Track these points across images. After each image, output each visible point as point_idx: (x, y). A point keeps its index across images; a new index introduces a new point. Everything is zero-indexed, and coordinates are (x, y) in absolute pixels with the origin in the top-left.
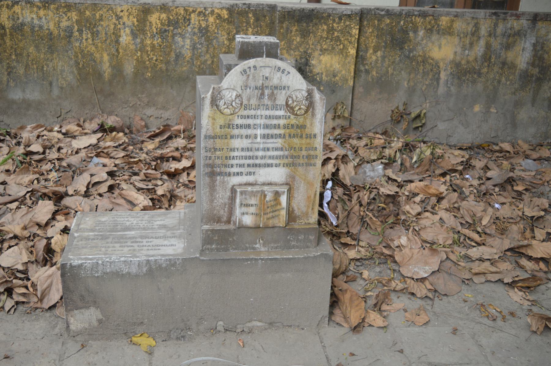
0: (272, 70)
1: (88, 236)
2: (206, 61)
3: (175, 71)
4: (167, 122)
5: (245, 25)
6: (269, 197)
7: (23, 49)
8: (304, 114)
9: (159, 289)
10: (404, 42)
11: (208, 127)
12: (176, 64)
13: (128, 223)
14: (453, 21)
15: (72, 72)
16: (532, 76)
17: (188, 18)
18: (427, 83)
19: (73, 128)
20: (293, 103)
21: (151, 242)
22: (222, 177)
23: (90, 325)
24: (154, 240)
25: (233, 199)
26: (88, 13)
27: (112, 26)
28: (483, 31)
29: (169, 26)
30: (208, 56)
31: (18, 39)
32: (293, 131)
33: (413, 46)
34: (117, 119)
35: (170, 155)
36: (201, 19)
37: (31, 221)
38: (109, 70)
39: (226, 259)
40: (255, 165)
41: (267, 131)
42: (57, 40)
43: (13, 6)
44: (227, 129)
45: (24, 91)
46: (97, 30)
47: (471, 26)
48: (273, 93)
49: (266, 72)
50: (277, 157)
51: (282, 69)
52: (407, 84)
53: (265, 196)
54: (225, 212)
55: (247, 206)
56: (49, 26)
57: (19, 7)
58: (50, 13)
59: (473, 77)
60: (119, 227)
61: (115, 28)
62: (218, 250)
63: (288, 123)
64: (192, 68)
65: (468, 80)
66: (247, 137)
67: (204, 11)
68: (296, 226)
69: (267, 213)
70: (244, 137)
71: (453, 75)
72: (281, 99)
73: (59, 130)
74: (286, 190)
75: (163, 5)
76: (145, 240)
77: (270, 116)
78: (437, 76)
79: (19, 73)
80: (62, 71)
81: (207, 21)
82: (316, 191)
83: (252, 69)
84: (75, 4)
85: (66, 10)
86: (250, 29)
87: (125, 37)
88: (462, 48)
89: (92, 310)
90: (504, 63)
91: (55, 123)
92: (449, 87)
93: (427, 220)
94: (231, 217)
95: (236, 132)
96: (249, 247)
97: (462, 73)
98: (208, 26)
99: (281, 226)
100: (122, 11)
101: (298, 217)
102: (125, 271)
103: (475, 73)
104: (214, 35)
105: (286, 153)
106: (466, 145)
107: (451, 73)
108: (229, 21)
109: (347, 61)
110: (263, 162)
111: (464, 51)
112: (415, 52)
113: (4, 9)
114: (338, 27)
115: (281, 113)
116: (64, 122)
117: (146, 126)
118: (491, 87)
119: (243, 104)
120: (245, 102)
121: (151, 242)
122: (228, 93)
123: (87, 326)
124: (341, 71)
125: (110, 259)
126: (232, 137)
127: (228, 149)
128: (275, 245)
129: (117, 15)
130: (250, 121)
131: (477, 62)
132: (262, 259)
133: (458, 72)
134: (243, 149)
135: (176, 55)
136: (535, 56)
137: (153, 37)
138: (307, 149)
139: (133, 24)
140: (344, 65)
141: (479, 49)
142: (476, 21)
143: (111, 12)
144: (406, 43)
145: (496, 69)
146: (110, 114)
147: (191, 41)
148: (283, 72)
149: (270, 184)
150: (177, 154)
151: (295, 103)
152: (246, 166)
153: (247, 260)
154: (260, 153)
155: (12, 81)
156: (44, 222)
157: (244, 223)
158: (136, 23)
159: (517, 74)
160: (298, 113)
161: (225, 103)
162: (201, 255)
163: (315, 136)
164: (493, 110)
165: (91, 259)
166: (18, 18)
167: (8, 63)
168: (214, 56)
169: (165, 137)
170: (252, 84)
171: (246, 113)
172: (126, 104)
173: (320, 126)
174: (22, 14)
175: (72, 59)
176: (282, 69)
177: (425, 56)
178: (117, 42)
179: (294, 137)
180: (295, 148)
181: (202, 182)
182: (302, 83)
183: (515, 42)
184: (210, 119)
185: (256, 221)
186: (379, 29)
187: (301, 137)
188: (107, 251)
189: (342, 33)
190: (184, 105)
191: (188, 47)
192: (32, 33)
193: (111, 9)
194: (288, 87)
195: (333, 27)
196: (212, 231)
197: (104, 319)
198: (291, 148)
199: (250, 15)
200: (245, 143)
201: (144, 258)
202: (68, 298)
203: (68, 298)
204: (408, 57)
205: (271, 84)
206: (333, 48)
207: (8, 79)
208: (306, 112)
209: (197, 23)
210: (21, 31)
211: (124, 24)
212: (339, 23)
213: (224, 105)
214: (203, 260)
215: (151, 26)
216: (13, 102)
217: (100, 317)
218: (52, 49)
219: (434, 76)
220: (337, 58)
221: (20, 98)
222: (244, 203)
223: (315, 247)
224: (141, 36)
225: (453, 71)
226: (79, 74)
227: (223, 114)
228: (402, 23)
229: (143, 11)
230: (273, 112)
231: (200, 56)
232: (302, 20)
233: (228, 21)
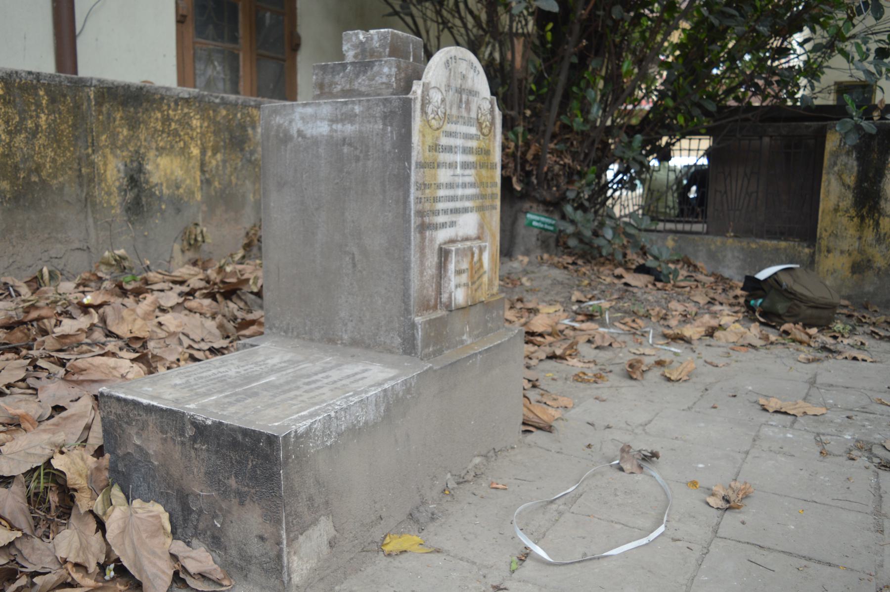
5: (33, 108)
25: (442, 266)
40: (456, 211)
52: (254, 197)
86: (42, 115)
109: (190, 165)
114: (175, 115)
124: (185, 180)
140: (187, 171)
189: (180, 124)
195: (168, 115)
199: (41, 93)
204: (250, 161)
206: (172, 147)
212: (175, 110)
220: (179, 160)
233: (5, 100)
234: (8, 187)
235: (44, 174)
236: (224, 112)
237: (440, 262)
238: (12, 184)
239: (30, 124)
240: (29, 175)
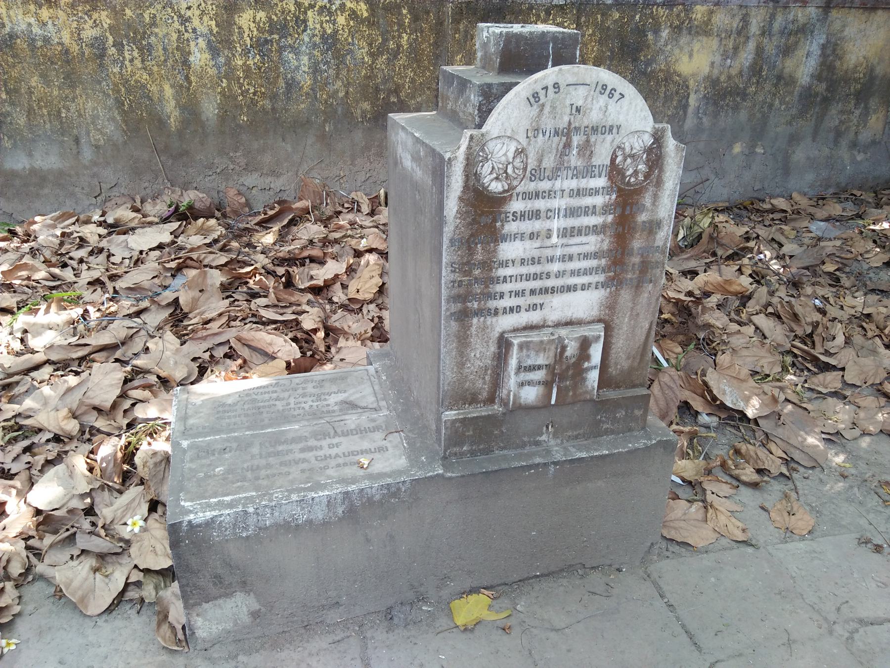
1: (209, 444)
2: (337, 91)
3: (287, 110)
4: (280, 195)
6: (572, 349)
7: (18, 80)
9: (368, 541)
10: (638, 50)
12: (289, 99)
13: (280, 405)
14: (711, 12)
15: (113, 119)
16: (817, 94)
18: (670, 113)
19: (124, 214)
21: (337, 445)
23: (236, 624)
24: (342, 439)
26: (128, 12)
27: (175, 36)
28: (754, 28)
33: (652, 56)
34: (201, 195)
35: (306, 253)
37: (81, 403)
38: (177, 113)
39: (492, 471)
40: (545, 291)
45: (30, 155)
47: (737, 19)
48: (588, 141)
49: (578, 96)
50: (586, 272)
51: (609, 88)
53: (564, 348)
54: (484, 383)
58: (61, 13)
59: (734, 100)
60: (265, 415)
61: (179, 38)
62: (473, 453)
64: (314, 105)
65: (727, 105)
66: (532, 236)
67: (328, 5)
70: (527, 236)
71: (707, 98)
73: (102, 219)
76: (325, 443)
77: (579, 190)
78: (684, 101)
79: (18, 124)
80: (95, 117)
83: (551, 90)
87: (198, 55)
88: (722, 55)
90: (779, 78)
91: (92, 207)
92: (701, 119)
93: (738, 336)
94: (495, 392)
97: (721, 94)
98: (336, 32)
100: (189, 8)
102: (303, 518)
103: (738, 94)
106: (722, 205)
107: (705, 96)
108: (371, 23)
111: (725, 60)
112: (654, 66)
116: (108, 204)
117: (248, 204)
118: (758, 115)
120: (532, 163)
121: (337, 445)
122: (499, 146)
123: (229, 626)
125: (271, 500)
129: (180, 16)
130: (540, 204)
131: (742, 76)
133: (715, 94)
134: (523, 262)
135: (286, 83)
136: (822, 64)
137: (246, 53)
139: (211, 31)
141: (746, 57)
142: (744, 12)
143: (170, 10)
144: (642, 50)
145: (768, 86)
146: (185, 187)
149: (569, 323)
150: (316, 252)
151: (629, 160)
152: (527, 293)
153: (529, 467)
154: (556, 267)
156: (108, 405)
157: (522, 401)
158: (215, 30)
159: (796, 93)
160: (633, 180)
161: (493, 168)
164: (759, 150)
165: (230, 505)
168: (349, 83)
169: (285, 222)
172: (210, 168)
173: (669, 204)
174: (9, 16)
175: (109, 95)
176: (609, 88)
177: (668, 71)
178: (186, 63)
181: (443, 332)
183: (797, 43)
186: (601, 28)
188: (257, 478)
190: (305, 167)
192: (33, 51)
194: (619, 127)
197: (263, 609)
201: (338, 489)
202: (188, 585)
203: (188, 585)
204: (644, 73)
205: (586, 124)
209: (318, 26)
210: (11, 47)
211: (194, 30)
213: (491, 173)
214: (450, 478)
215: (241, 34)
216: (14, 174)
217: (256, 606)
218: (71, 80)
219: (681, 101)
221: (25, 168)
224: (226, 52)
225: (708, 93)
226: (125, 121)
228: (637, 17)
230: (584, 181)
231: (326, 85)
232: (489, 17)
233: (369, 22)
234: (369, 107)
235: (403, 94)
236: (617, 15)
237: (500, 354)
238: (373, 105)
239: (392, 45)
240: (388, 96)
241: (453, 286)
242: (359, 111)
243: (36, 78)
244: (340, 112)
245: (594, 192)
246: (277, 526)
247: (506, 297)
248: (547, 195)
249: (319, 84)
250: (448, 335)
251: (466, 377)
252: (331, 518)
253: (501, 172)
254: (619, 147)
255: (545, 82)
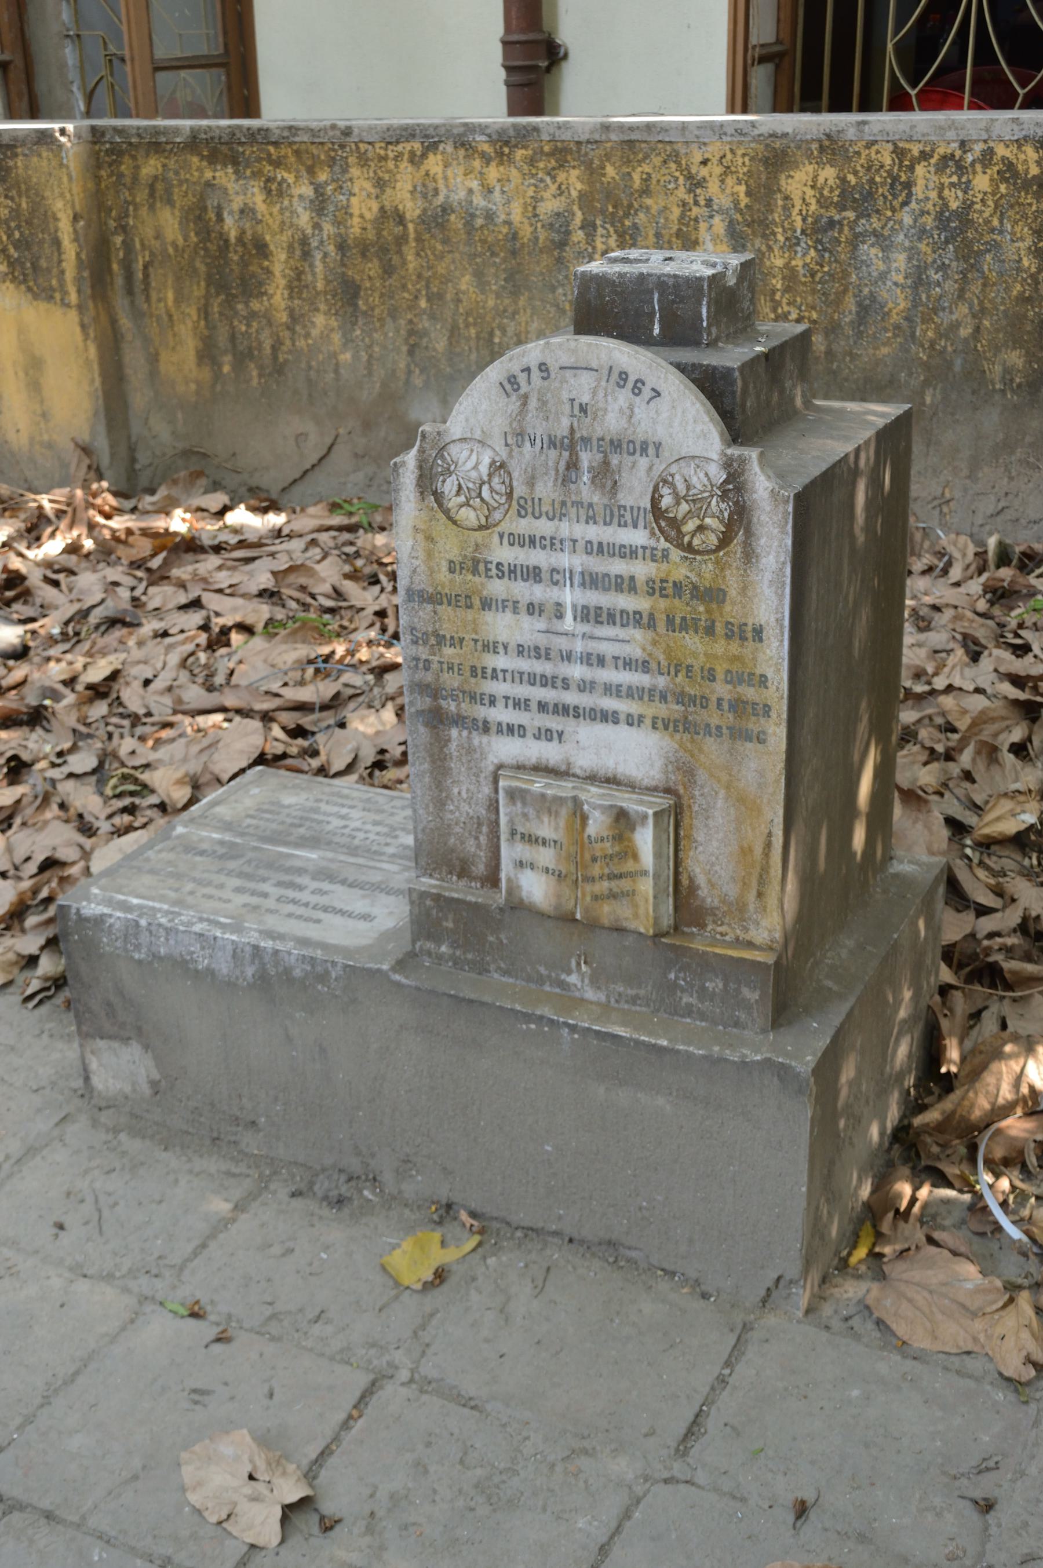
0: (599, 380)
2: (955, 326)
3: (853, 357)
6: (597, 824)
7: (446, 280)
8: (719, 548)
9: (289, 1039)
11: (416, 563)
12: (860, 334)
17: (903, 178)
20: (678, 503)
22: (465, 733)
23: (134, 1090)
26: (610, 170)
27: (676, 212)
29: (844, 209)
30: (964, 309)
31: (433, 249)
32: (680, 608)
36: (946, 181)
39: (464, 999)
40: (563, 710)
41: (594, 598)
42: (529, 254)
43: (424, 156)
44: (470, 577)
46: (635, 226)
48: (606, 463)
49: (582, 387)
50: (631, 693)
51: (632, 379)
53: (584, 818)
54: (479, 846)
55: (530, 841)
56: (508, 214)
57: (439, 157)
58: (514, 172)
61: (683, 216)
63: (663, 575)
64: (907, 351)
66: (532, 609)
67: (958, 154)
68: (698, 945)
69: (593, 879)
72: (635, 491)
74: (650, 812)
75: (828, 136)
77: (600, 544)
79: (435, 350)
81: (967, 187)
82: (770, 834)
83: (536, 374)
84: (579, 143)
85: (553, 163)
89: (134, 1051)
95: (497, 588)
96: (549, 976)
98: (968, 206)
99: (642, 930)
100: (705, 162)
101: (712, 911)
102: (203, 964)
104: (987, 238)
105: (662, 682)
110: (585, 700)
113: (404, 164)
115: (638, 537)
119: (515, 496)
120: (520, 490)
123: (128, 1089)
126: (487, 604)
127: (476, 641)
128: (631, 992)
129: (690, 177)
130: (537, 557)
132: (573, 1028)
134: (521, 650)
135: (859, 304)
137: (791, 243)
138: (732, 678)
139: (736, 203)
143: (673, 166)
147: (910, 259)
148: (637, 390)
149: (612, 781)
151: (684, 507)
153: (528, 1018)
154: (577, 671)
155: (417, 371)
157: (524, 894)
158: (744, 201)
160: (696, 542)
161: (460, 485)
162: (393, 969)
163: (758, 633)
166: (436, 192)
167: (411, 322)
168: (983, 310)
170: (537, 426)
171: (524, 526)
173: (774, 597)
174: (446, 178)
176: (632, 379)
179: (684, 627)
180: (689, 668)
182: (704, 435)
184: (420, 537)
185: (559, 897)
187: (710, 631)
191: (900, 279)
192: (469, 233)
193: (675, 156)
194: (658, 446)
196: (437, 898)
198: (677, 667)
200: (527, 630)
205: (599, 433)
207: (408, 365)
208: (725, 541)
209: (933, 195)
210: (442, 226)
211: (709, 202)
213: (458, 494)
214: (398, 984)
215: (787, 209)
217: (156, 1075)
218: (515, 283)
222: (520, 829)
223: (764, 1031)
224: (758, 242)
227: (455, 523)
229: (766, 161)
231: (935, 311)
234: (1020, 363)
241: (416, 666)
242: (998, 368)
243: (467, 277)
244: (958, 363)
245: (629, 553)
246: (169, 957)
247: (500, 704)
248: (548, 543)
249: (922, 310)
250: (416, 746)
251: (449, 826)
252: (237, 978)
253: (474, 494)
254: (665, 481)
255: (525, 360)
